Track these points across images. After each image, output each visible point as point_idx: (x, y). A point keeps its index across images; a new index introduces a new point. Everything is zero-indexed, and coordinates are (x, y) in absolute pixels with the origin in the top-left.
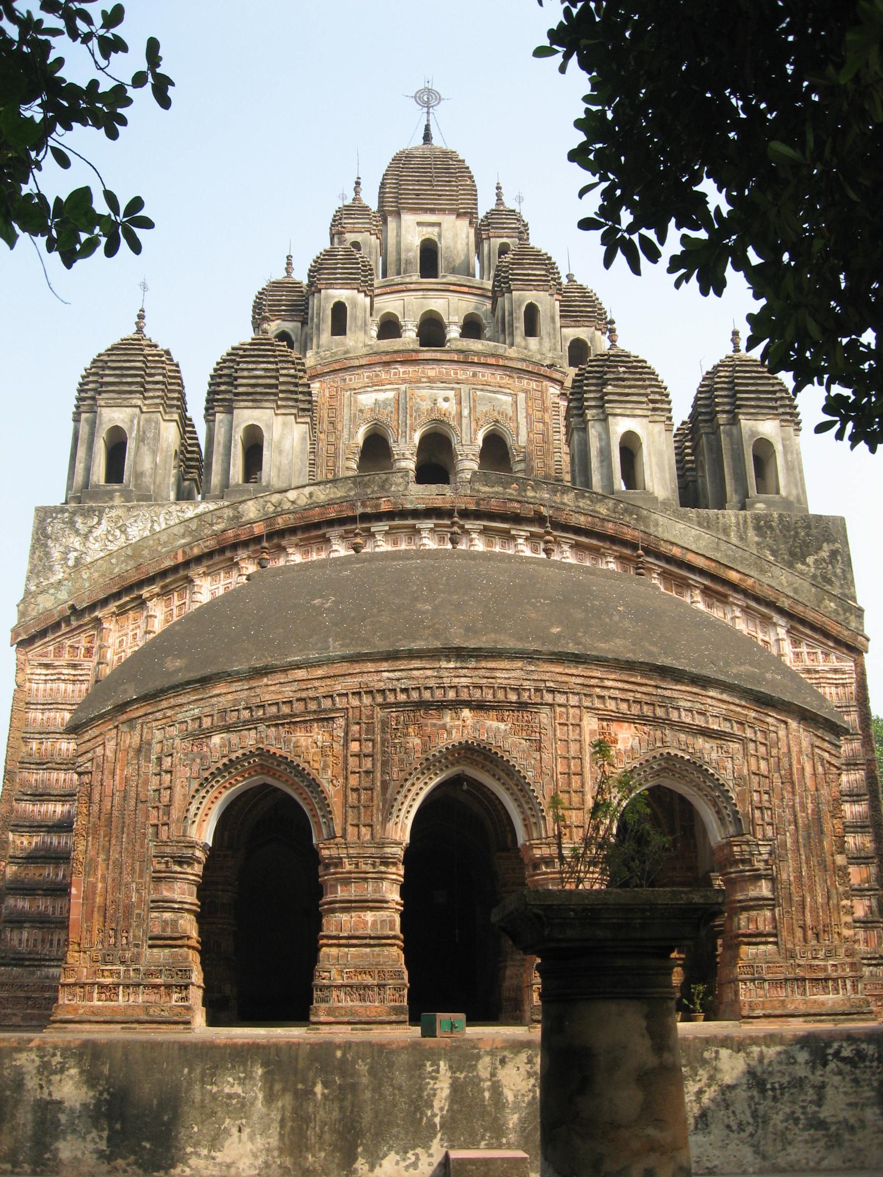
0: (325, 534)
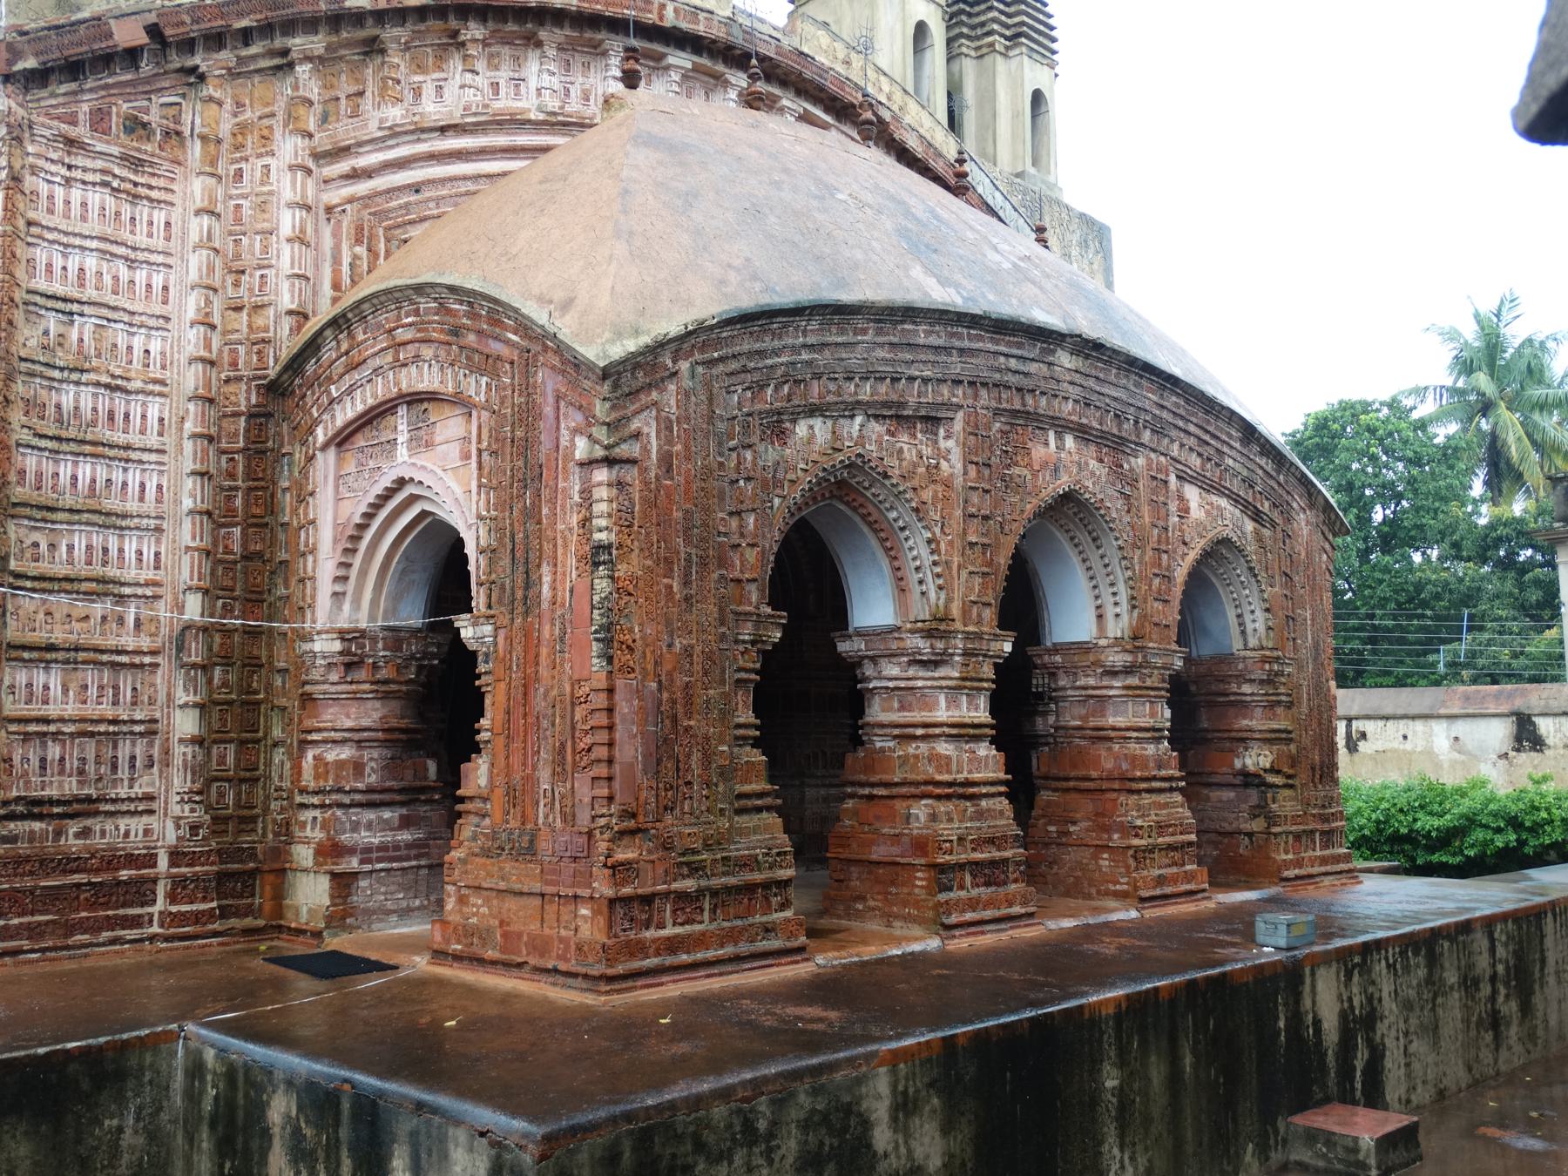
0: (601, 42)
